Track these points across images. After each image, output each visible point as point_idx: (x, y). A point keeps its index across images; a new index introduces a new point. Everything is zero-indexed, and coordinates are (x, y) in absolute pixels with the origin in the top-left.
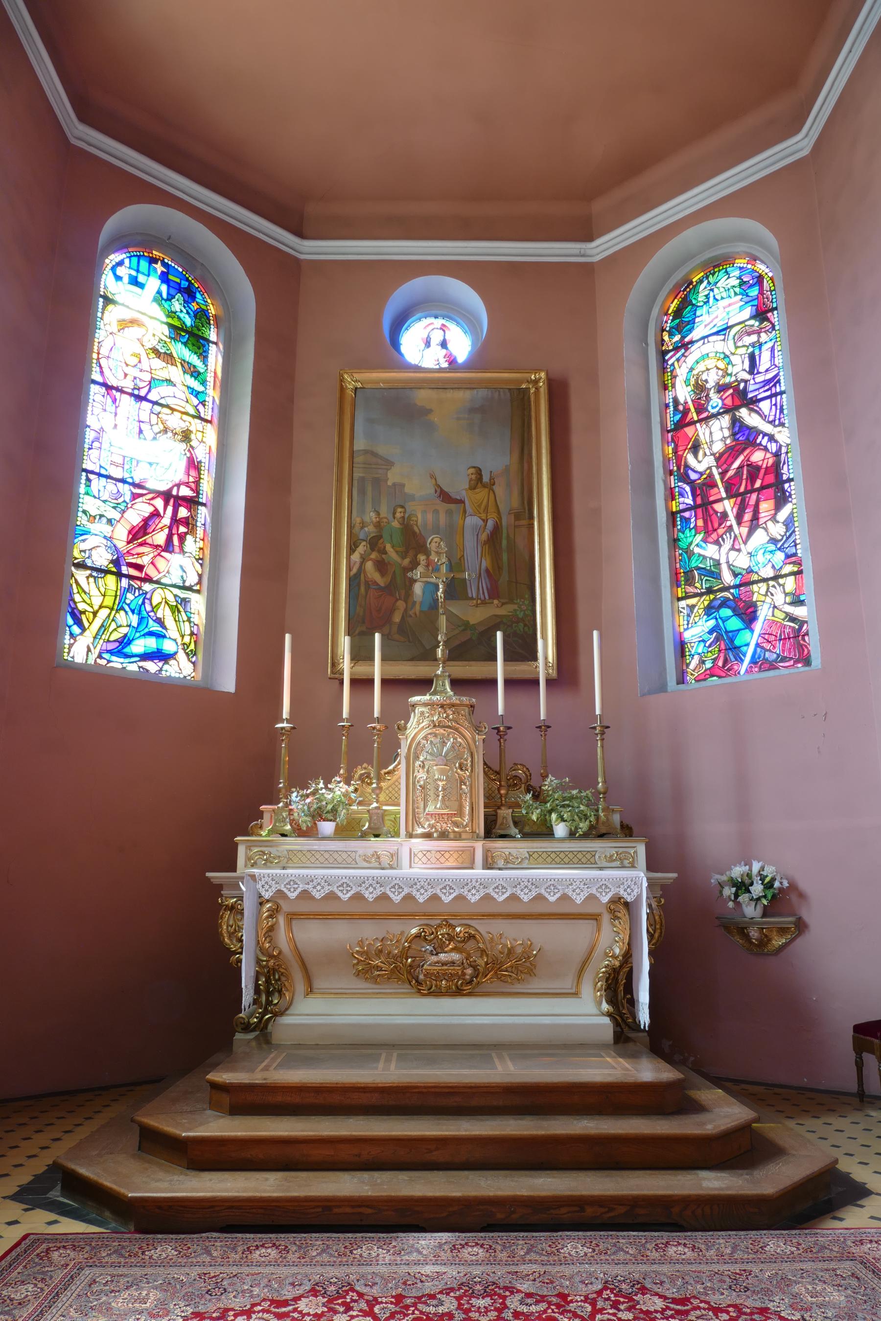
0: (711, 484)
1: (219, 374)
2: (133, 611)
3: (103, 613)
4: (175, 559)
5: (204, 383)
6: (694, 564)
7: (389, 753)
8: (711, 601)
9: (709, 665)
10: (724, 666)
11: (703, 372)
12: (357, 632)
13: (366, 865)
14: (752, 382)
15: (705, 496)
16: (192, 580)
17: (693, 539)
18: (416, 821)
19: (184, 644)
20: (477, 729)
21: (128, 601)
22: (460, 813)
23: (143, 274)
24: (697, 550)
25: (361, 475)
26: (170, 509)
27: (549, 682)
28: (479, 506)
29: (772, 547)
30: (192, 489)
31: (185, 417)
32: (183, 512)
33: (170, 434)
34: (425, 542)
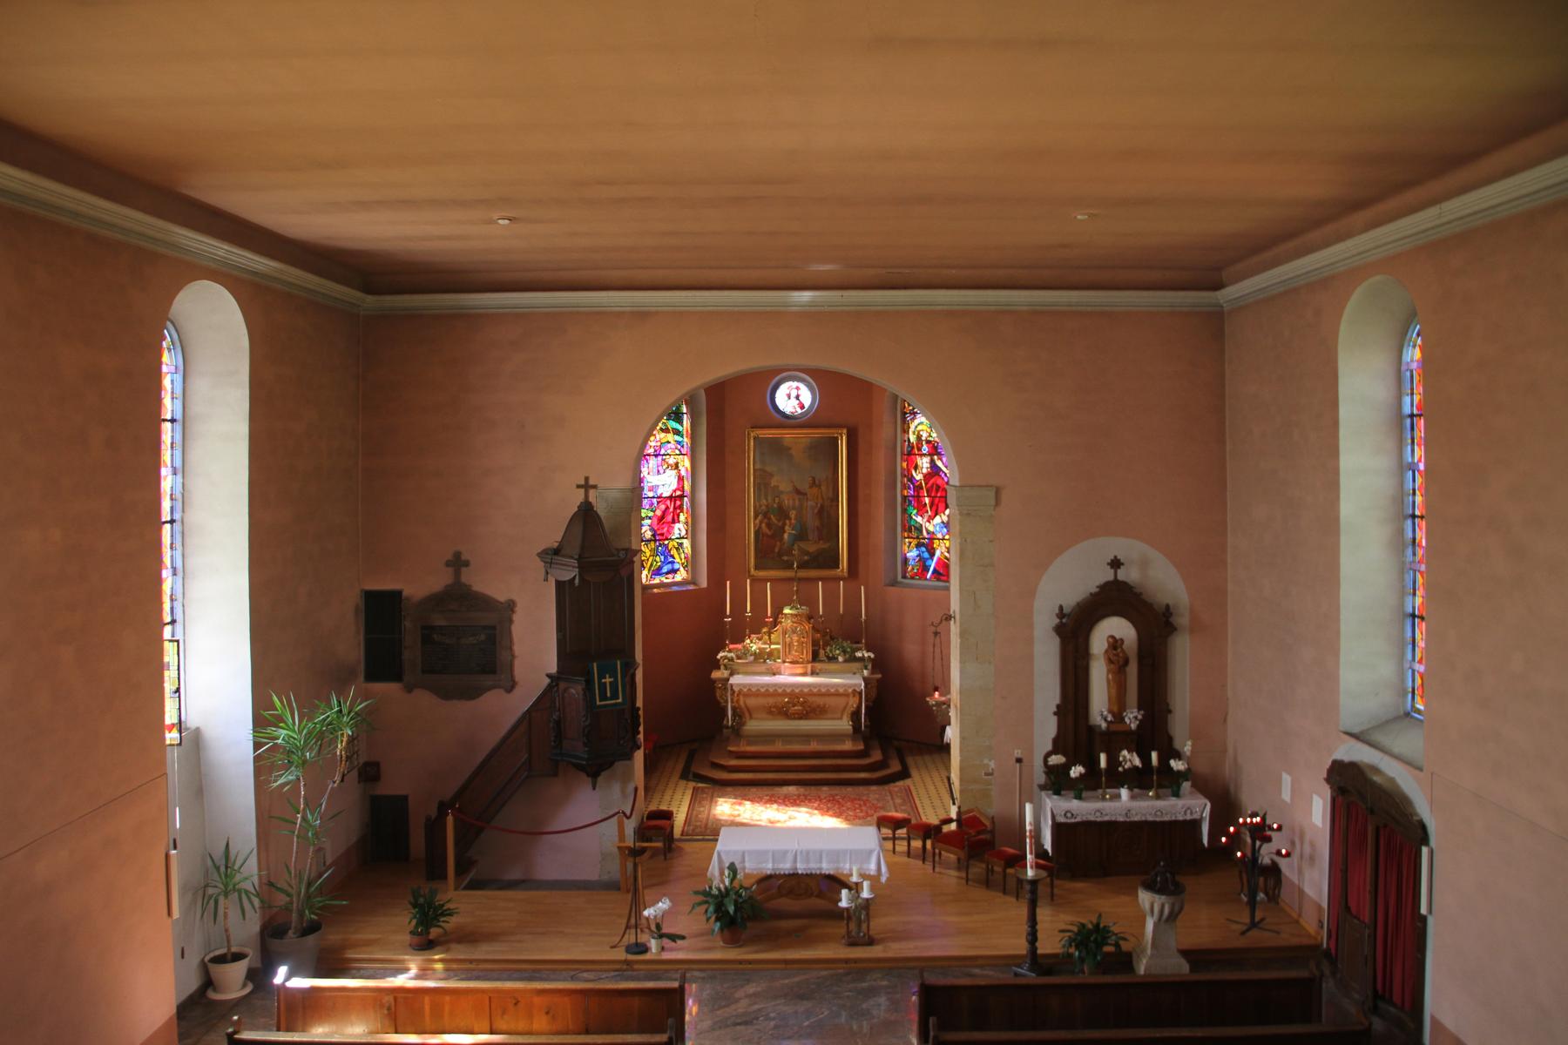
4: (677, 526)
7: (775, 623)
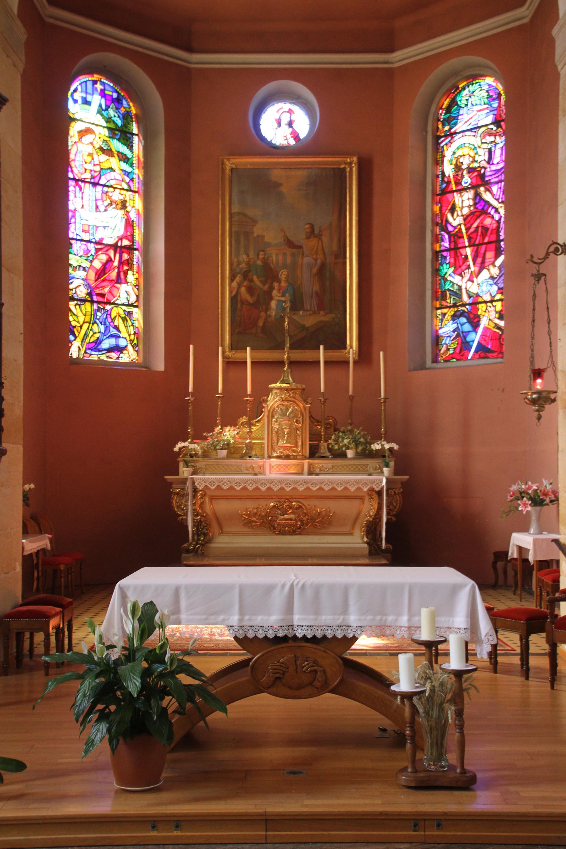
0: (459, 235)
1: (142, 159)
2: (101, 323)
3: (86, 326)
4: (123, 287)
5: (132, 165)
6: (447, 287)
8: (456, 312)
9: (451, 351)
10: (460, 353)
11: (461, 156)
12: (236, 332)
13: (246, 472)
14: (488, 169)
15: (456, 243)
16: (133, 299)
17: (447, 270)
18: (273, 450)
19: (131, 340)
20: (306, 401)
21: (98, 317)
22: (296, 446)
23: (90, 94)
24: (449, 278)
25: (236, 229)
26: (118, 255)
27: (355, 362)
28: (312, 250)
29: (491, 282)
30: (129, 241)
31: (123, 192)
32: (125, 256)
33: (114, 206)
34: (278, 274)
